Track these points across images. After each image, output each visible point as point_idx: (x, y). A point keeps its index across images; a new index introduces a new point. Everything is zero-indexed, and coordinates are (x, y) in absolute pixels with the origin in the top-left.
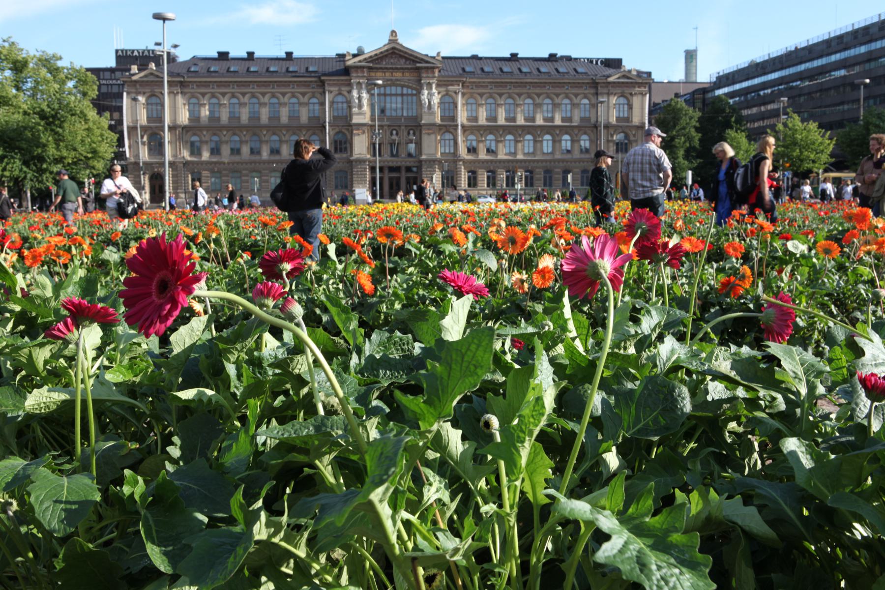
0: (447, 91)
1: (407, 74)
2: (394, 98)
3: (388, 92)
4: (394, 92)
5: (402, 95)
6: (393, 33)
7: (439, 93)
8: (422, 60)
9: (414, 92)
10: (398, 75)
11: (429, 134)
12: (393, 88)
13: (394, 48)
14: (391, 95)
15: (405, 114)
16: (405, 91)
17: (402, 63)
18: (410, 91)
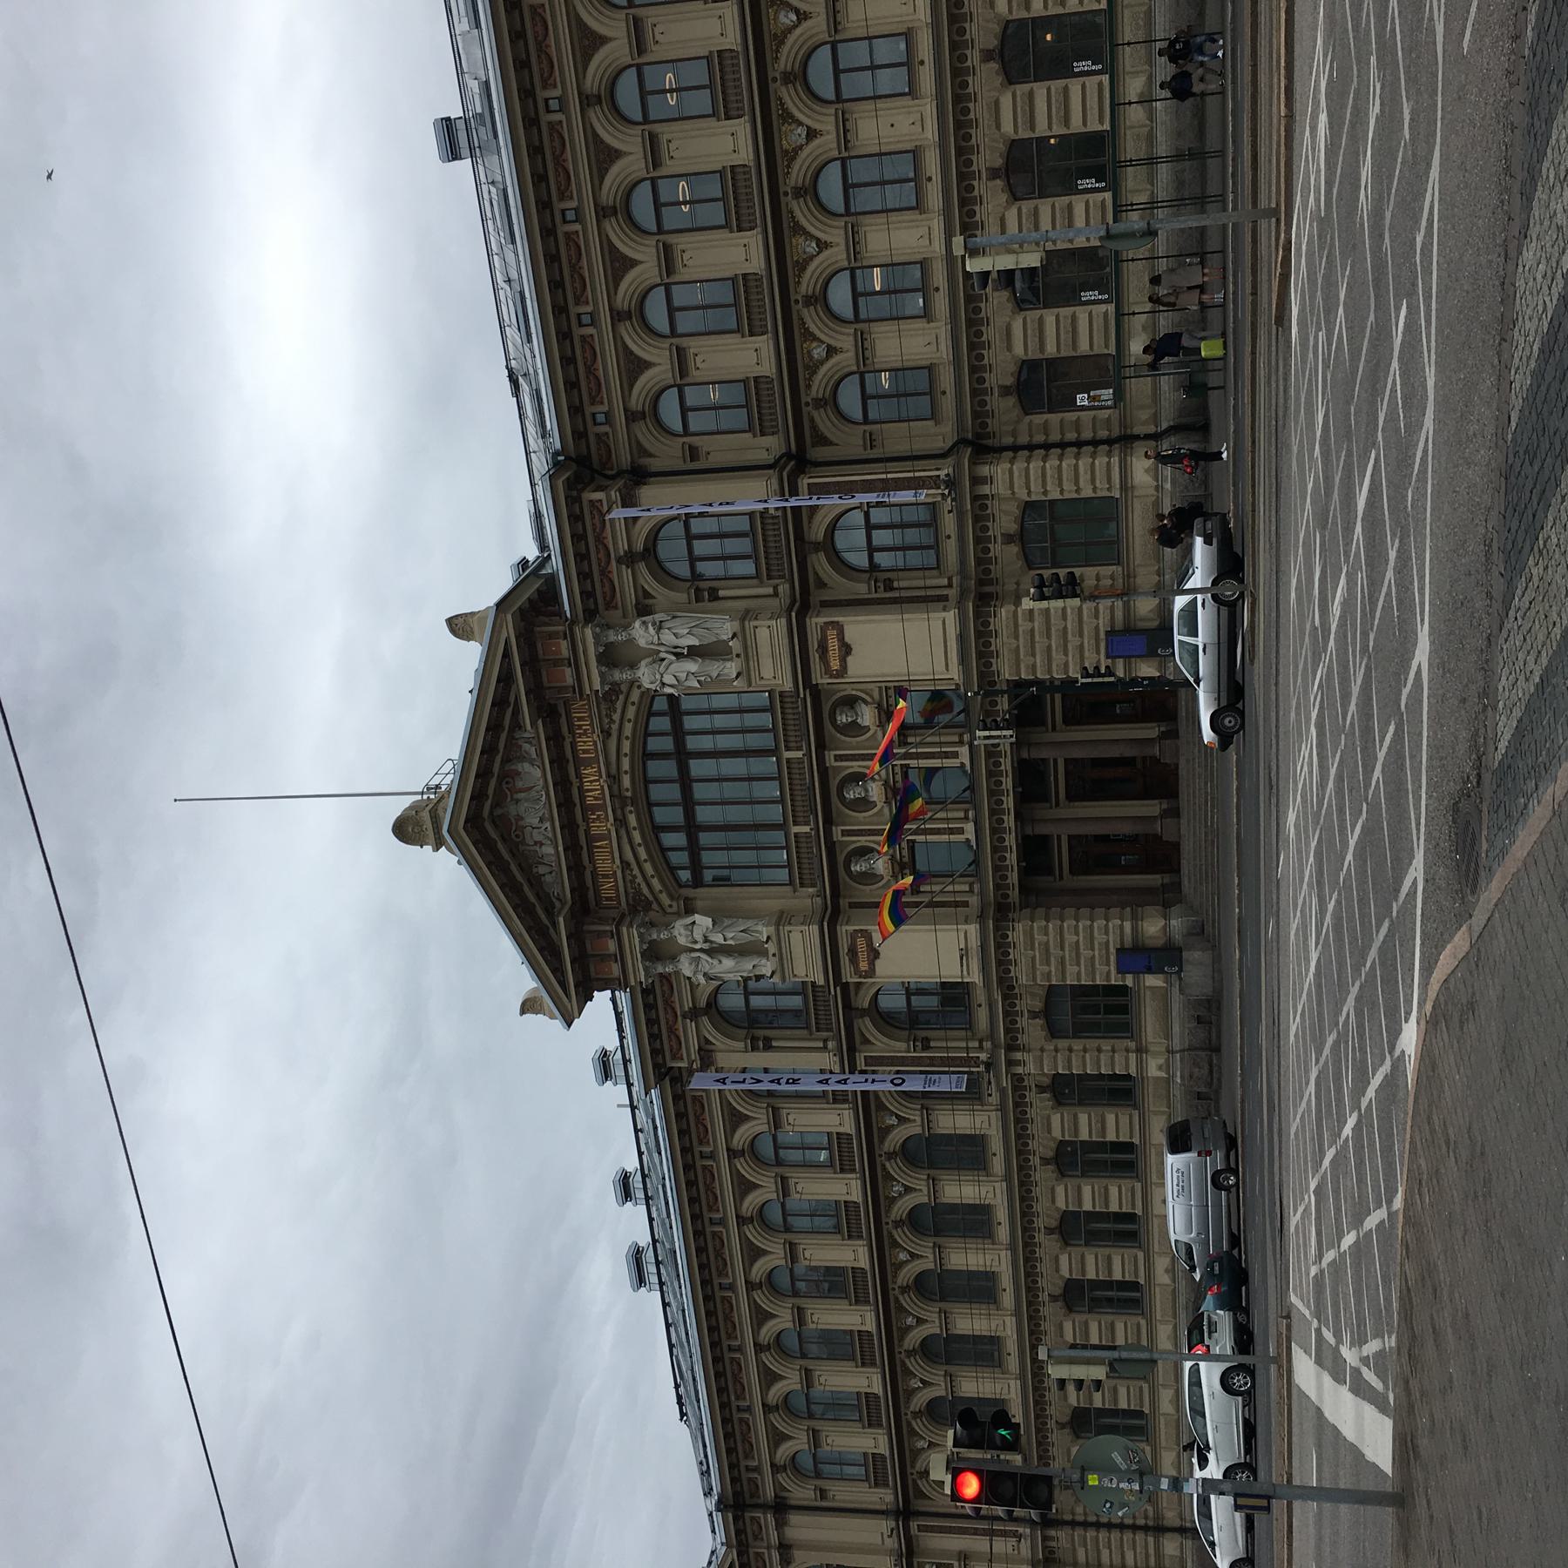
0: (630, 559)
1: (587, 745)
2: (700, 791)
3: (676, 815)
4: (674, 792)
5: (682, 756)
6: (406, 829)
7: (644, 610)
8: (500, 703)
9: (661, 704)
10: (594, 783)
11: (846, 649)
12: (657, 792)
13: (474, 823)
14: (688, 803)
15: (766, 741)
16: (667, 744)
17: (535, 774)
18: (662, 723)
